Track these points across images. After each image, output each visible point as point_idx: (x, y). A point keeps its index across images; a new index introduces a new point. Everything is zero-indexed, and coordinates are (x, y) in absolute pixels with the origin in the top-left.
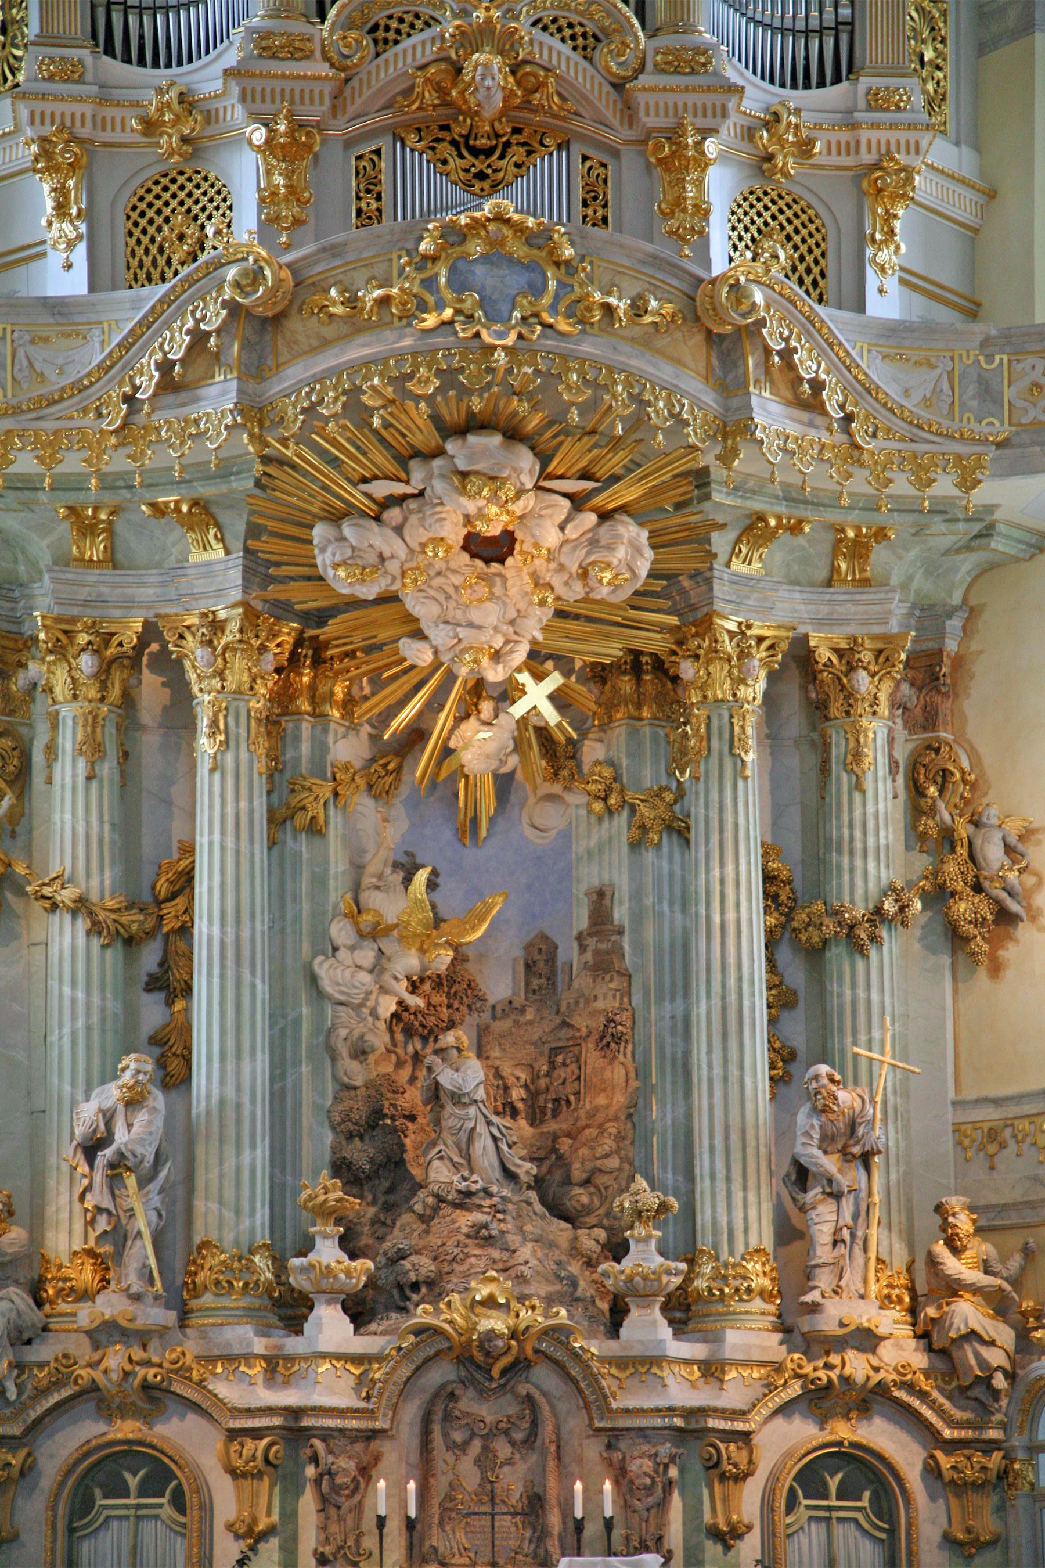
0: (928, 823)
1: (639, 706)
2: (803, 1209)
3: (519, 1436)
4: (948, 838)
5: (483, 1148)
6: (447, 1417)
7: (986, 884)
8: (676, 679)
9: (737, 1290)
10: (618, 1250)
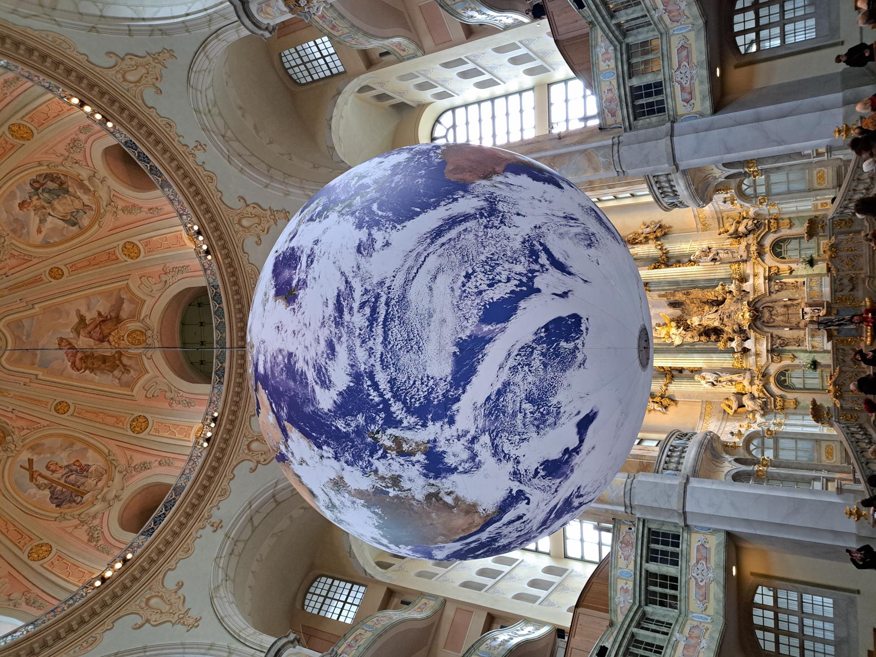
4: (645, 237)
10: (730, 292)
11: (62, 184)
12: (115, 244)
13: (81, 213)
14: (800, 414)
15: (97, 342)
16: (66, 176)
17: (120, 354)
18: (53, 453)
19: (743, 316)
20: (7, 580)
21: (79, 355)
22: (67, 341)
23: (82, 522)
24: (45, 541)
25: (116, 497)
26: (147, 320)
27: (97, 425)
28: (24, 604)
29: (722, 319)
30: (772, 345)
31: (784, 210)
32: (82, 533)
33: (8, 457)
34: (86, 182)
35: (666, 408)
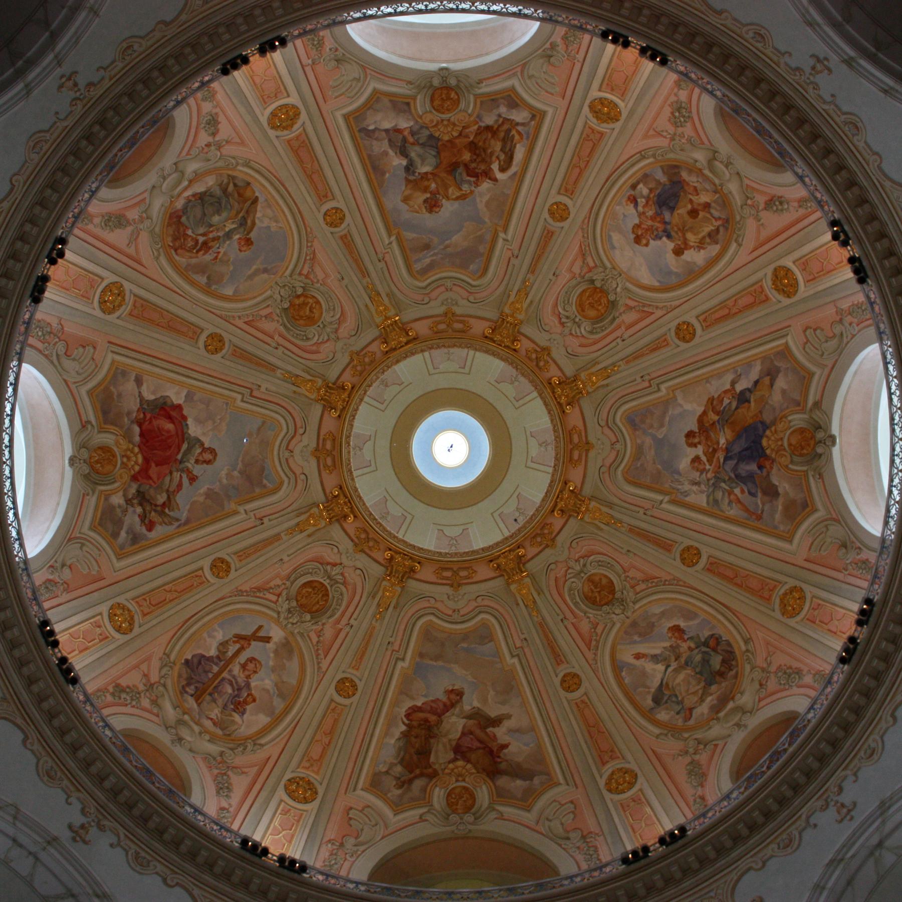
11: (721, 674)
12: (629, 757)
13: (678, 708)
15: (454, 743)
16: (736, 676)
17: (434, 775)
18: (273, 670)
20: (94, 573)
21: (433, 718)
22: (458, 702)
23: (152, 685)
24: (136, 630)
25: (180, 739)
26: (493, 815)
27: (310, 732)
28: (51, 577)
32: (134, 679)
33: (279, 613)
34: (731, 705)
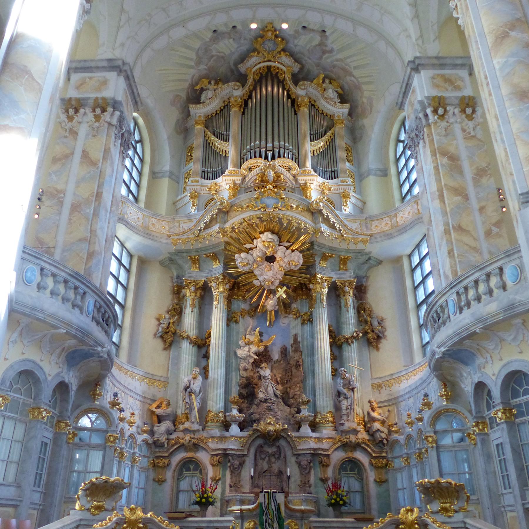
0: (361, 319)
1: (302, 296)
2: (340, 402)
3: (277, 456)
4: (366, 322)
5: (270, 389)
6: (261, 452)
7: (375, 330)
8: (310, 290)
9: (325, 421)
10: (299, 412)
14: (146, 485)
19: (270, 423)
29: (266, 401)
30: (232, 455)
31: (399, 475)
35: (161, 337)
